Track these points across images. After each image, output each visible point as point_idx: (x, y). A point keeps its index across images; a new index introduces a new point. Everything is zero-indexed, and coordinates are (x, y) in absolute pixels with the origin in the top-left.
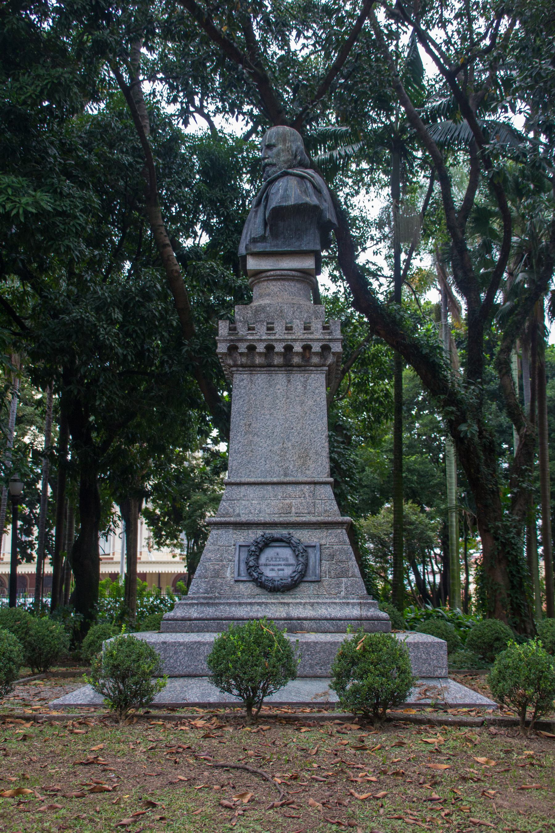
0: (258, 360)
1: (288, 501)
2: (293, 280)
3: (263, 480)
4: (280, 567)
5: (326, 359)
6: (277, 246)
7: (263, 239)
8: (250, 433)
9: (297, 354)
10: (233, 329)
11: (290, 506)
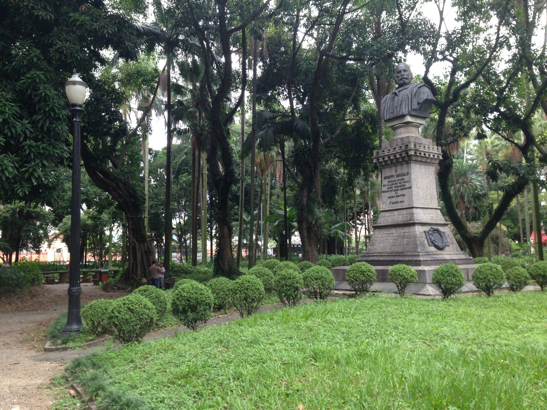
7: (416, 110)
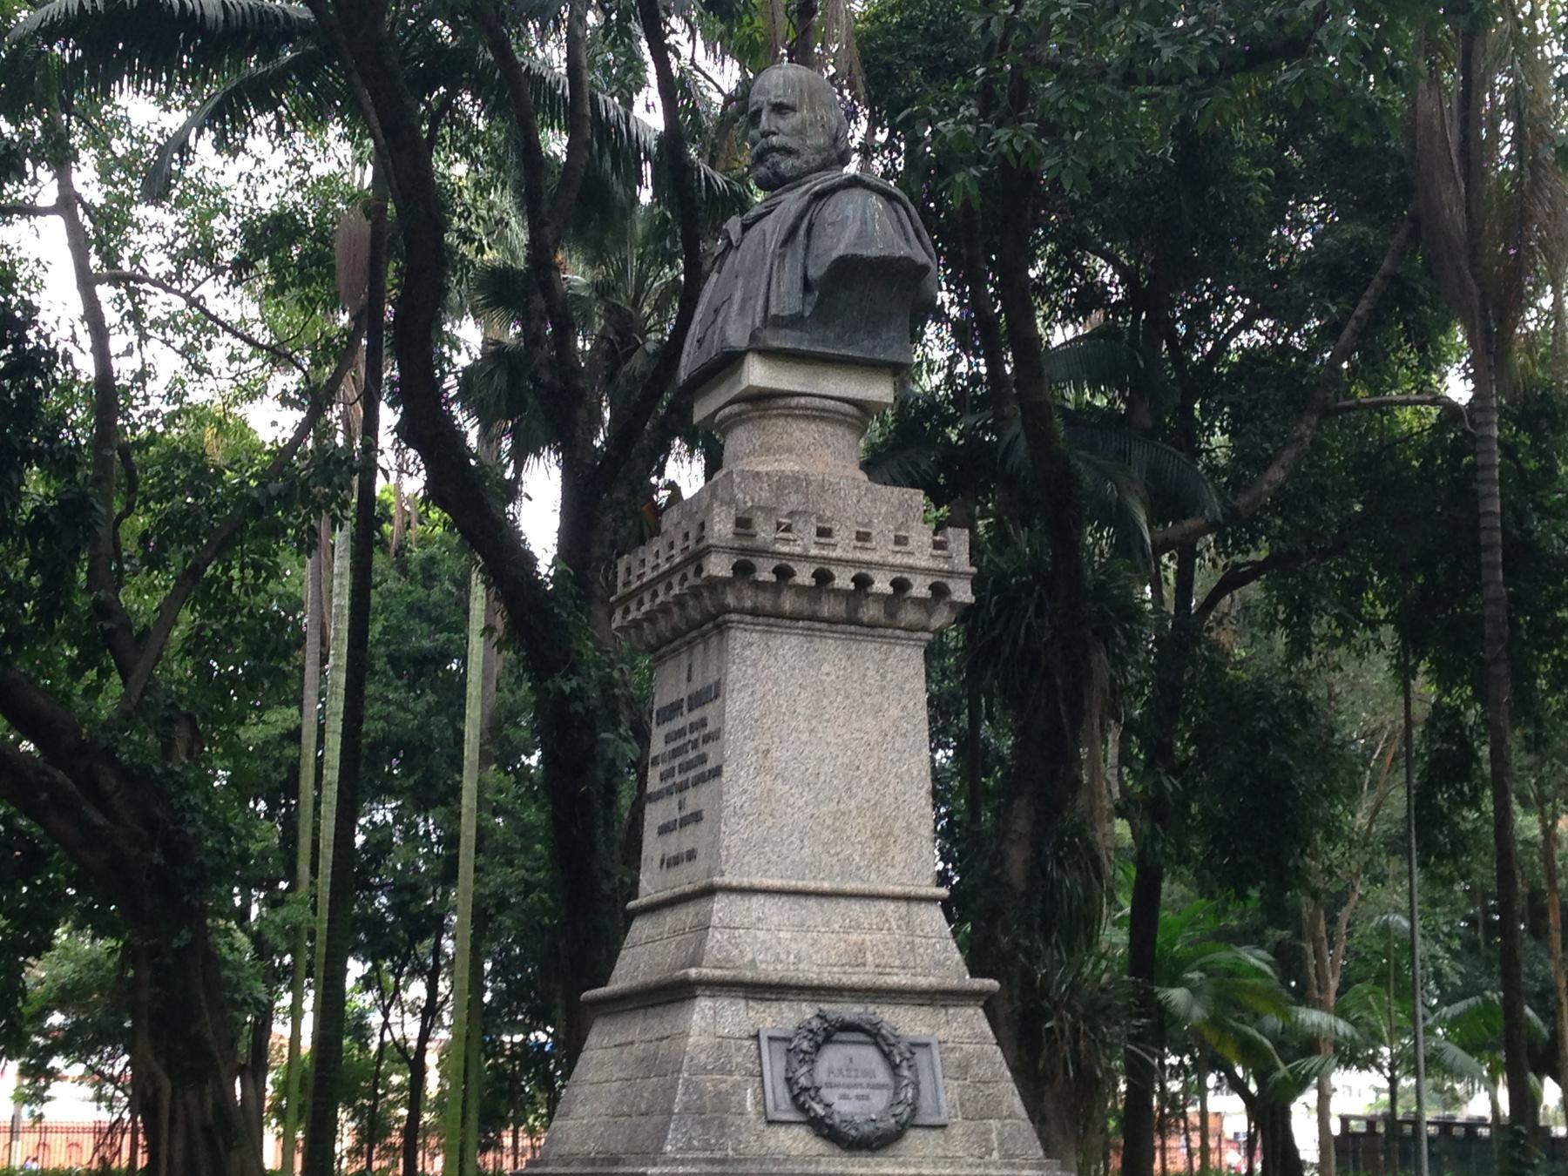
0: (788, 603)
1: (854, 937)
2: (841, 423)
3: (800, 884)
4: (859, 1091)
5: (930, 615)
6: (823, 341)
7: (794, 322)
8: (768, 771)
9: (880, 597)
11: (861, 949)
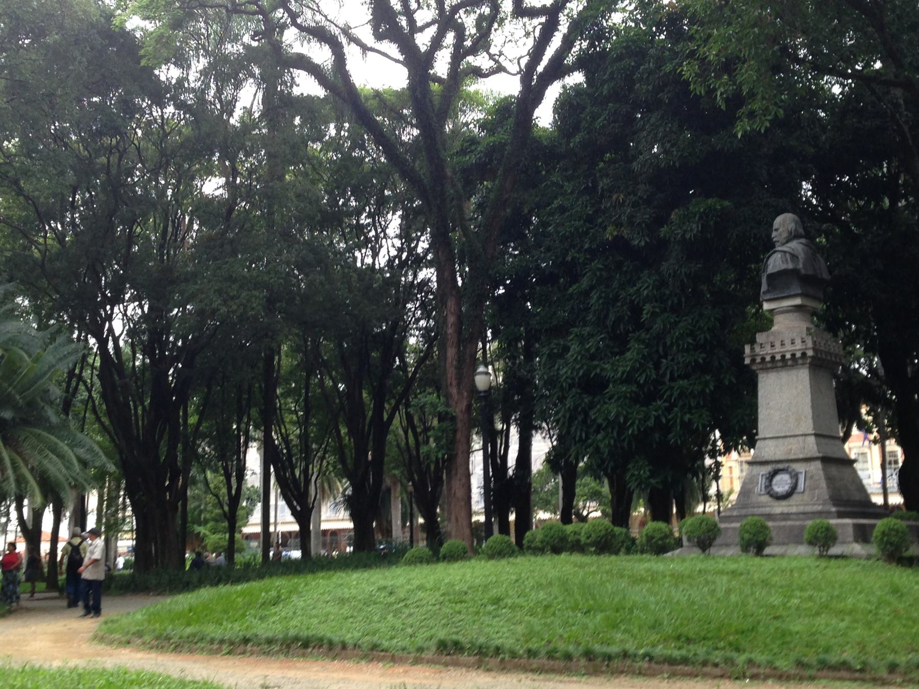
0: (769, 365)
10: (752, 349)
11: (791, 450)
